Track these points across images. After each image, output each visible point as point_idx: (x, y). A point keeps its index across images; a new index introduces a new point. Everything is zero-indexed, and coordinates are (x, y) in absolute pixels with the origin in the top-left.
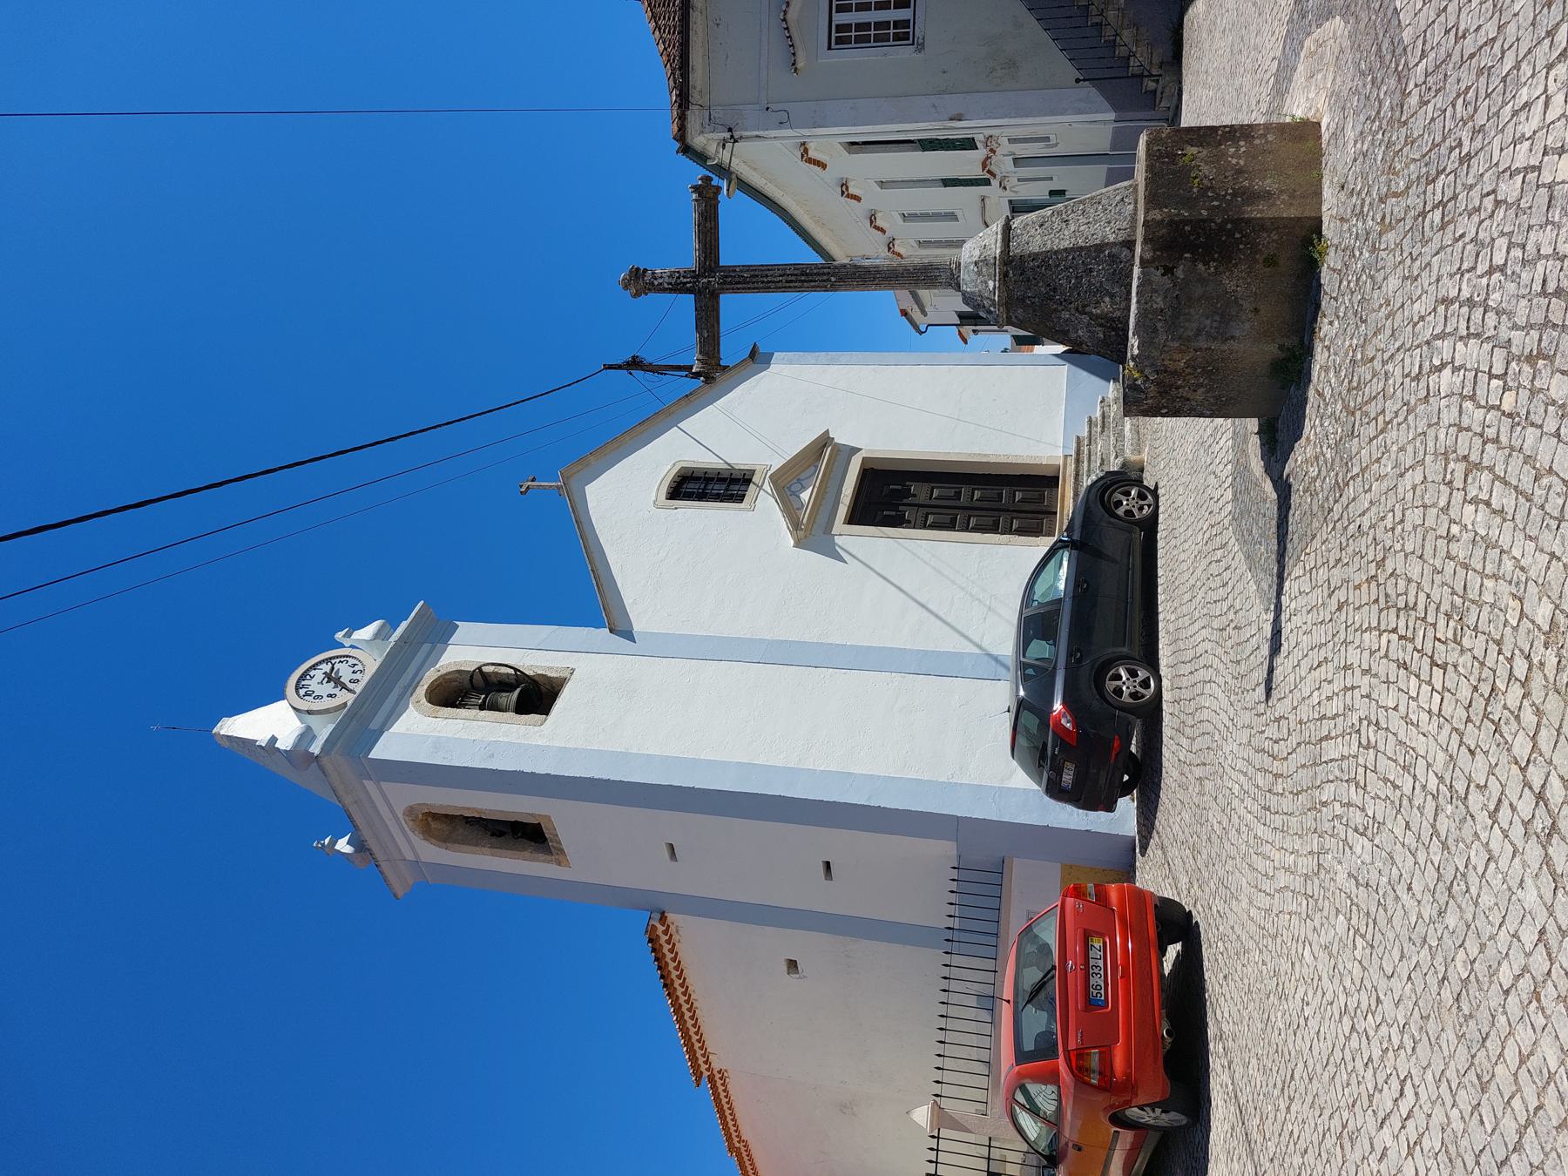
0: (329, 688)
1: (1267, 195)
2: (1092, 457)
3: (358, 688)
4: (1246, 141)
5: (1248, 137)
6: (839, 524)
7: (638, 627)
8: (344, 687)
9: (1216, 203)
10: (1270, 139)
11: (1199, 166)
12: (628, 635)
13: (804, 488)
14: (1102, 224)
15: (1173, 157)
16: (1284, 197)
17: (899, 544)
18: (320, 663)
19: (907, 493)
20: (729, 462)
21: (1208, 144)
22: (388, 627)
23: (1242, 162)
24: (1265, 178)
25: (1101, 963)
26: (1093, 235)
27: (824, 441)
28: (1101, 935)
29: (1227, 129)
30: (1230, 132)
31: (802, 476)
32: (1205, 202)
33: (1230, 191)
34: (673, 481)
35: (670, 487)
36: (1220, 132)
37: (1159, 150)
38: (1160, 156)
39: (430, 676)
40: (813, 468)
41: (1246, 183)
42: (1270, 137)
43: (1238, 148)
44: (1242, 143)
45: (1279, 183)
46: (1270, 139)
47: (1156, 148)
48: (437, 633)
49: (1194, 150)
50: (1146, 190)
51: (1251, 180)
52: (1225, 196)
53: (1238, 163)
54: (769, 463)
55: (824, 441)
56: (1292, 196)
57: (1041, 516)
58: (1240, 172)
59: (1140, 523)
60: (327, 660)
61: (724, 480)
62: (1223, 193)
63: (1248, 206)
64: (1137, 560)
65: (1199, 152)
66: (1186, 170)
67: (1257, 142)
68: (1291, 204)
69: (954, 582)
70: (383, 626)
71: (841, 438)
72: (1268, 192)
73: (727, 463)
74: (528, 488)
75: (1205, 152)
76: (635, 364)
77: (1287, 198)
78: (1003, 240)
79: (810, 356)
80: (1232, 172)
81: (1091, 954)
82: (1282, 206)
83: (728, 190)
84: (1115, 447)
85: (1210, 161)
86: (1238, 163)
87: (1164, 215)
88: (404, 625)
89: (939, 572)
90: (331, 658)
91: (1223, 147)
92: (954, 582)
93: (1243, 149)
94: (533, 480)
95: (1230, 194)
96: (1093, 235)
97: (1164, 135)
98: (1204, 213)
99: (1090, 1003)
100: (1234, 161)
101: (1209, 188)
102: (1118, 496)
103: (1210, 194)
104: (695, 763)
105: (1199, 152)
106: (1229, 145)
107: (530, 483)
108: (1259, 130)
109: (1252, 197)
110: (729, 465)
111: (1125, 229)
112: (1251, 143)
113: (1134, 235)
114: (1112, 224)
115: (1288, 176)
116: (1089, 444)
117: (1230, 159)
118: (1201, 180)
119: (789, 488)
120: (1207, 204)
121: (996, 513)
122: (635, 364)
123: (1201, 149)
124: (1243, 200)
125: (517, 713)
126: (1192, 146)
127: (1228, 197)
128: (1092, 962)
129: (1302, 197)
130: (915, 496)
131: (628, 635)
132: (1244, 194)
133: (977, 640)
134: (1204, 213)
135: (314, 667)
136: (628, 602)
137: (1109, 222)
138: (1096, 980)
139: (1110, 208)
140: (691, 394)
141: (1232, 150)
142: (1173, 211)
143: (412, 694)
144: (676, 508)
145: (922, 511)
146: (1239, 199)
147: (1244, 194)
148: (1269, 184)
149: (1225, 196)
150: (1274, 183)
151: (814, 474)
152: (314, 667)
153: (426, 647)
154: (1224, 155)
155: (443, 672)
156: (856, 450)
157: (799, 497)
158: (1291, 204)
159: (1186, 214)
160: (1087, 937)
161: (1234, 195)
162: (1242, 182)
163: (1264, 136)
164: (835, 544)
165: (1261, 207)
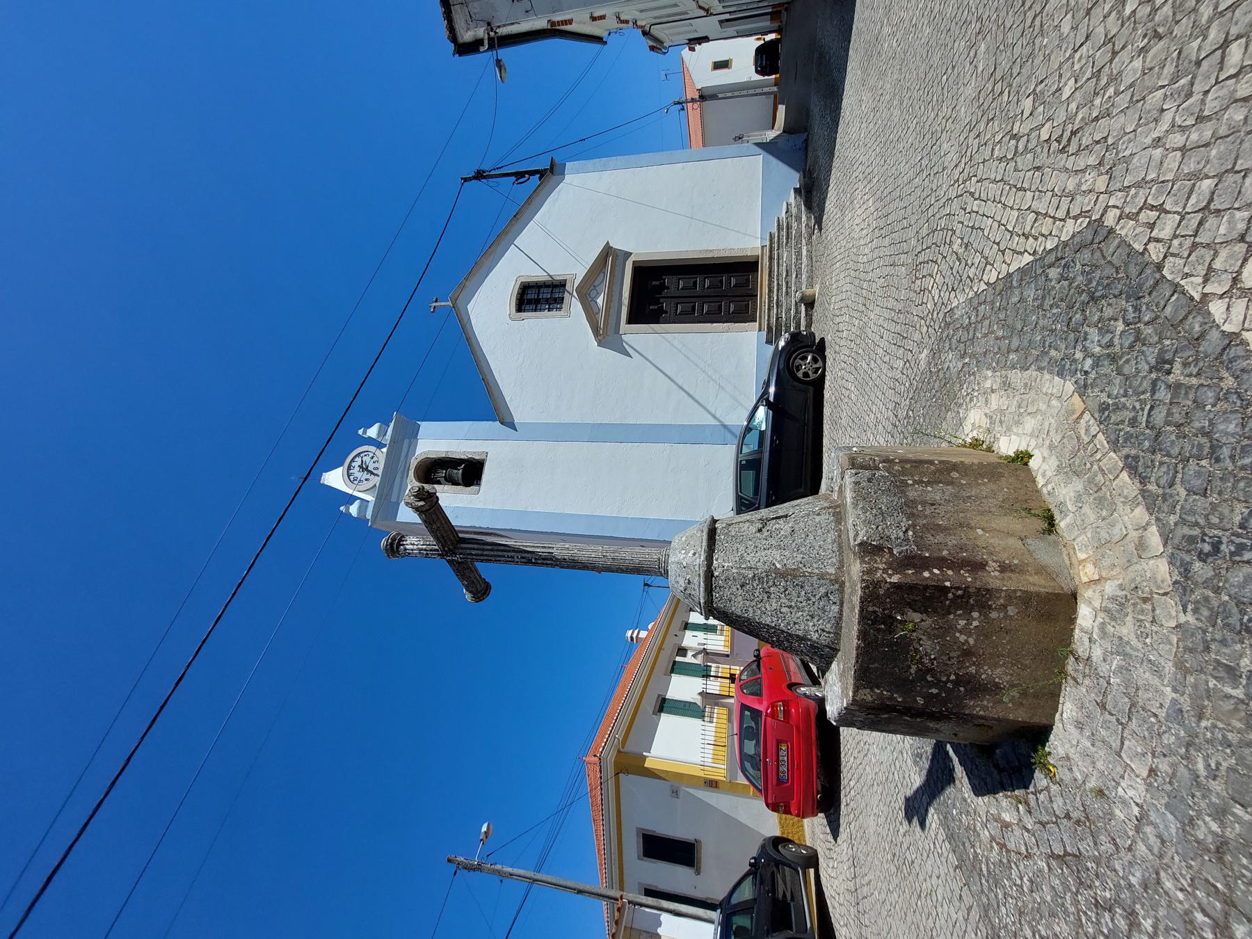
0: (365, 475)
1: (994, 689)
2: (781, 261)
3: (380, 472)
4: (980, 613)
5: (984, 608)
6: (624, 326)
7: (517, 419)
8: (372, 473)
9: (934, 691)
10: (1011, 613)
11: (920, 639)
12: (512, 426)
13: (598, 294)
14: (805, 614)
15: (890, 621)
16: (1015, 693)
17: (663, 337)
18: (355, 457)
19: (663, 287)
21: (935, 611)
22: (384, 426)
23: (971, 641)
24: (996, 666)
25: (786, 759)
26: (795, 623)
27: (608, 251)
28: (786, 742)
29: (960, 592)
30: (961, 597)
31: (596, 284)
32: (922, 687)
33: (953, 677)
34: (518, 294)
35: (517, 299)
36: (950, 595)
37: (875, 612)
38: (875, 622)
39: (414, 463)
40: (602, 274)
41: (973, 670)
42: (1012, 611)
43: (970, 620)
44: (975, 614)
45: (1011, 675)
46: (1011, 613)
47: (870, 609)
48: (408, 434)
49: (917, 617)
50: (857, 662)
51: (978, 665)
52: (946, 683)
53: (966, 641)
54: (574, 272)
55: (608, 251)
56: (1024, 694)
57: (747, 298)
58: (967, 653)
59: (813, 383)
60: (358, 455)
61: (548, 286)
62: (944, 679)
63: (971, 698)
64: (810, 415)
65: (922, 620)
66: (905, 643)
67: (994, 615)
68: (1021, 704)
69: (697, 365)
70: (380, 427)
71: (616, 245)
72: (997, 685)
73: (549, 275)
74: (435, 307)
75: (929, 621)
76: (479, 175)
77: (1017, 695)
78: (706, 589)
79: (589, 163)
80: (958, 653)
81: (781, 753)
82: (1010, 705)
83: (501, 77)
85: (934, 635)
86: (966, 641)
87: (875, 698)
88: (392, 425)
89: (688, 358)
90: (360, 453)
91: (952, 616)
92: (697, 365)
93: (975, 623)
94: (436, 301)
95: (952, 681)
96: (795, 623)
97: (882, 592)
98: (920, 701)
99: (780, 782)
100: (962, 638)
101: (930, 671)
102: (798, 361)
103: (929, 678)
104: (563, 516)
105: (922, 620)
106: (960, 615)
107: (434, 304)
108: (999, 598)
109: (977, 688)
110: (551, 276)
111: (829, 633)
112: (986, 617)
113: (838, 644)
114: (815, 620)
115: (1025, 667)
116: (778, 249)
117: (958, 635)
118: (921, 658)
119: (589, 295)
120: (924, 690)
121: (719, 299)
122: (479, 175)
123: (924, 616)
124: (966, 690)
125: (466, 486)
126: (915, 611)
127: (949, 685)
128: (781, 758)
129: (1036, 696)
130: (668, 288)
131: (512, 426)
132: (969, 682)
133: (713, 412)
134: (920, 701)
135: (353, 460)
137: (812, 617)
138: (784, 768)
139: (813, 599)
140: (517, 214)
141: (962, 622)
142: (885, 693)
143: (407, 476)
145: (673, 301)
146: (962, 689)
147: (969, 682)
148: (998, 674)
149: (946, 683)
150: (1006, 674)
151: (603, 280)
152: (353, 460)
153: (406, 441)
154: (952, 628)
155: (419, 459)
156: (628, 254)
157: (596, 302)
158: (1021, 704)
159: (900, 700)
160: (778, 742)
161: (957, 683)
162: (968, 667)
163: (1004, 607)
164: (622, 340)
165: (985, 703)
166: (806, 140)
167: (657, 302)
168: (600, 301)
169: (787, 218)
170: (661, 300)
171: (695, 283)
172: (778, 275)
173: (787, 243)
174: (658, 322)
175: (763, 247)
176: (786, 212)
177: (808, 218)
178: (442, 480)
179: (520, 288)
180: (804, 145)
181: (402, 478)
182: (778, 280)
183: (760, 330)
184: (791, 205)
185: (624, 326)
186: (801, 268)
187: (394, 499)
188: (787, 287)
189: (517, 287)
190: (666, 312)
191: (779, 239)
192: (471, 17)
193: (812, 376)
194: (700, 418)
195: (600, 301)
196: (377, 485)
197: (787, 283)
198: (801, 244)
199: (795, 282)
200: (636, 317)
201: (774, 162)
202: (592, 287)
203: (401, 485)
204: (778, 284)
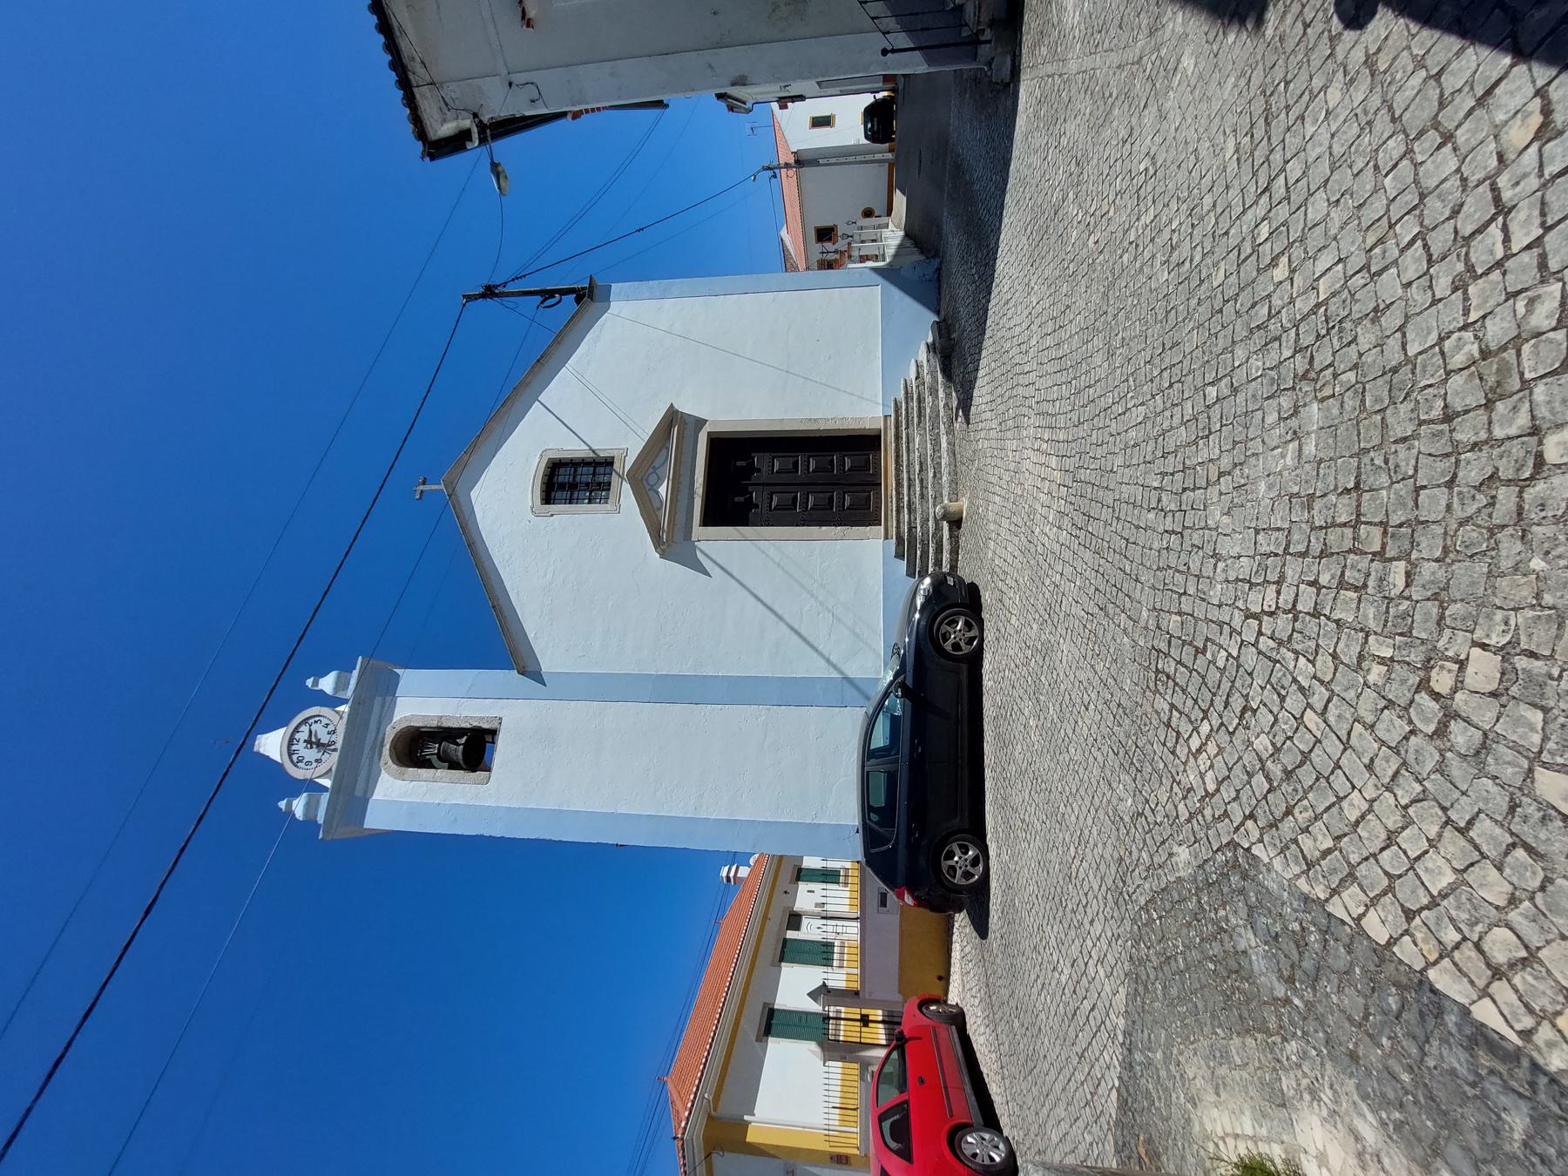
2: (911, 445)
6: (698, 530)
7: (546, 667)
13: (659, 481)
17: (756, 545)
19: (751, 469)
20: (594, 448)
27: (673, 418)
31: (657, 464)
34: (544, 475)
35: (543, 483)
39: (390, 734)
40: (664, 451)
48: (379, 690)
54: (624, 446)
55: (673, 418)
57: (868, 488)
60: (305, 721)
69: (802, 586)
70: (338, 678)
71: (685, 408)
73: (591, 449)
74: (422, 491)
76: (489, 292)
79: (644, 286)
83: (499, 188)
84: (932, 460)
88: (356, 673)
92: (802, 586)
102: (945, 628)
107: (421, 488)
110: (594, 451)
116: (907, 428)
119: (647, 480)
121: (829, 488)
122: (489, 292)
131: (537, 676)
136: (531, 636)
140: (542, 357)
143: (380, 759)
144: (552, 515)
153: (378, 701)
155: (398, 729)
156: (701, 423)
157: (657, 493)
166: (939, 270)
167: (744, 491)
168: (662, 490)
169: (917, 387)
170: (750, 488)
171: (796, 464)
172: (908, 466)
173: (919, 422)
174: (746, 524)
175: (886, 417)
176: (916, 378)
177: (948, 395)
178: (434, 759)
179: (547, 467)
180: (936, 276)
181: (371, 765)
182: (908, 472)
183: (886, 538)
184: (922, 366)
185: (698, 530)
186: (939, 464)
187: (359, 792)
188: (922, 487)
189: (543, 465)
190: (756, 506)
191: (907, 413)
192: (446, 104)
193: (966, 649)
194: (813, 668)
195: (662, 490)
196: (334, 769)
197: (921, 481)
198: (938, 428)
199: (933, 484)
200: (710, 519)
201: (896, 293)
202: (651, 470)
203: (370, 771)
204: (909, 479)
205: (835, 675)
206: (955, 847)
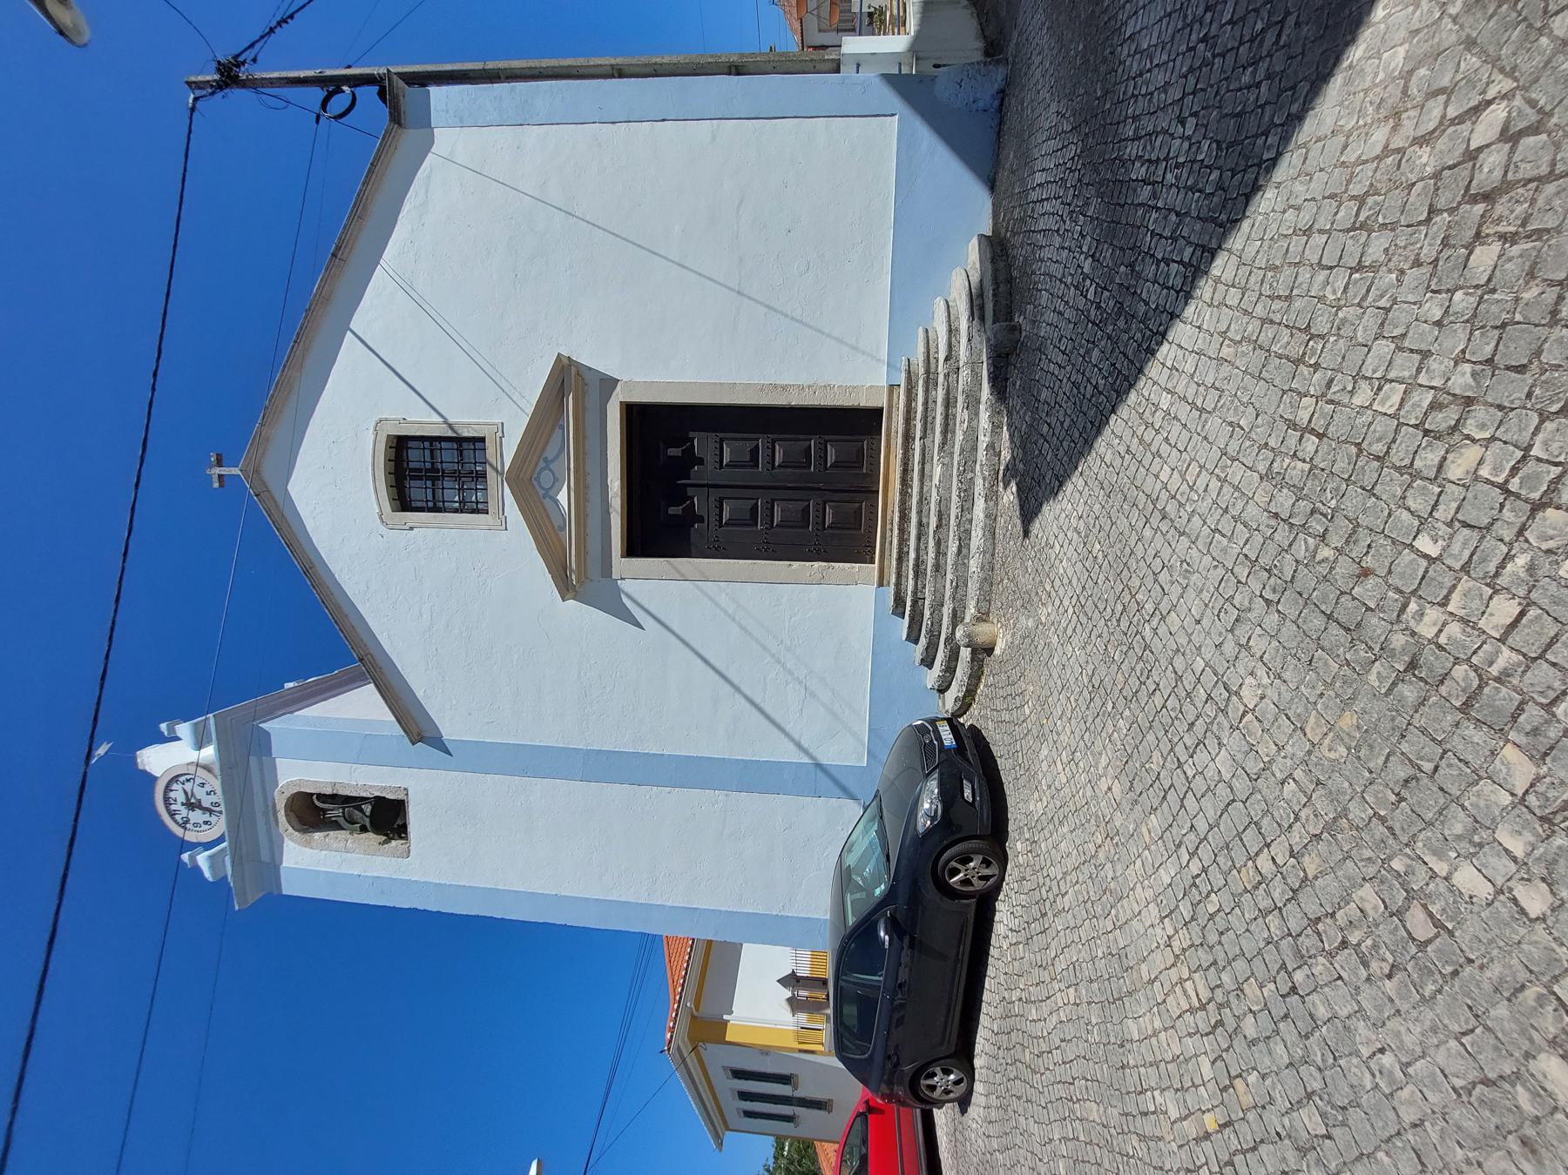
7: (448, 733)
13: (556, 483)
17: (698, 587)
19: (691, 459)
20: (451, 420)
31: (550, 453)
34: (388, 460)
40: (558, 431)
69: (764, 648)
73: (446, 422)
84: (958, 526)
92: (764, 648)
110: (450, 426)
119: (538, 479)
136: (420, 694)
140: (338, 248)
143: (277, 825)
144: (411, 529)
145: (715, 494)
155: (288, 794)
156: (609, 384)
157: (557, 502)
164: (619, 590)
166: (1002, 94)
167: (681, 496)
168: (562, 498)
169: (947, 376)
170: (690, 491)
171: (754, 452)
172: (920, 502)
173: (944, 443)
174: (687, 554)
175: (891, 387)
176: (947, 359)
177: (996, 428)
178: (341, 821)
179: (389, 447)
180: (997, 103)
181: (269, 831)
182: (920, 512)
183: (881, 584)
184: (957, 330)
185: (622, 565)
186: (968, 532)
187: (265, 856)
188: (938, 553)
189: (382, 447)
190: (701, 519)
191: (926, 409)
193: (978, 885)
195: (562, 498)
196: (226, 834)
197: (938, 544)
198: (973, 471)
199: (956, 564)
200: (636, 546)
201: (925, 137)
202: (542, 464)
203: (271, 842)
204: (920, 524)
205: (806, 760)
206: (938, 1070)
